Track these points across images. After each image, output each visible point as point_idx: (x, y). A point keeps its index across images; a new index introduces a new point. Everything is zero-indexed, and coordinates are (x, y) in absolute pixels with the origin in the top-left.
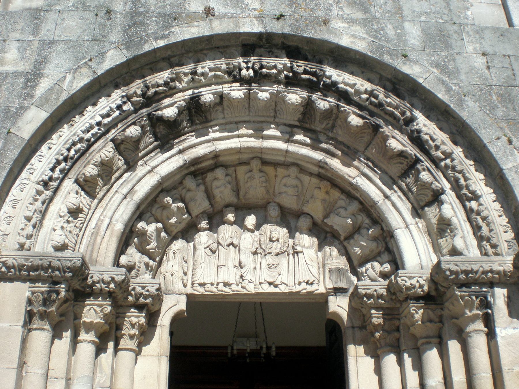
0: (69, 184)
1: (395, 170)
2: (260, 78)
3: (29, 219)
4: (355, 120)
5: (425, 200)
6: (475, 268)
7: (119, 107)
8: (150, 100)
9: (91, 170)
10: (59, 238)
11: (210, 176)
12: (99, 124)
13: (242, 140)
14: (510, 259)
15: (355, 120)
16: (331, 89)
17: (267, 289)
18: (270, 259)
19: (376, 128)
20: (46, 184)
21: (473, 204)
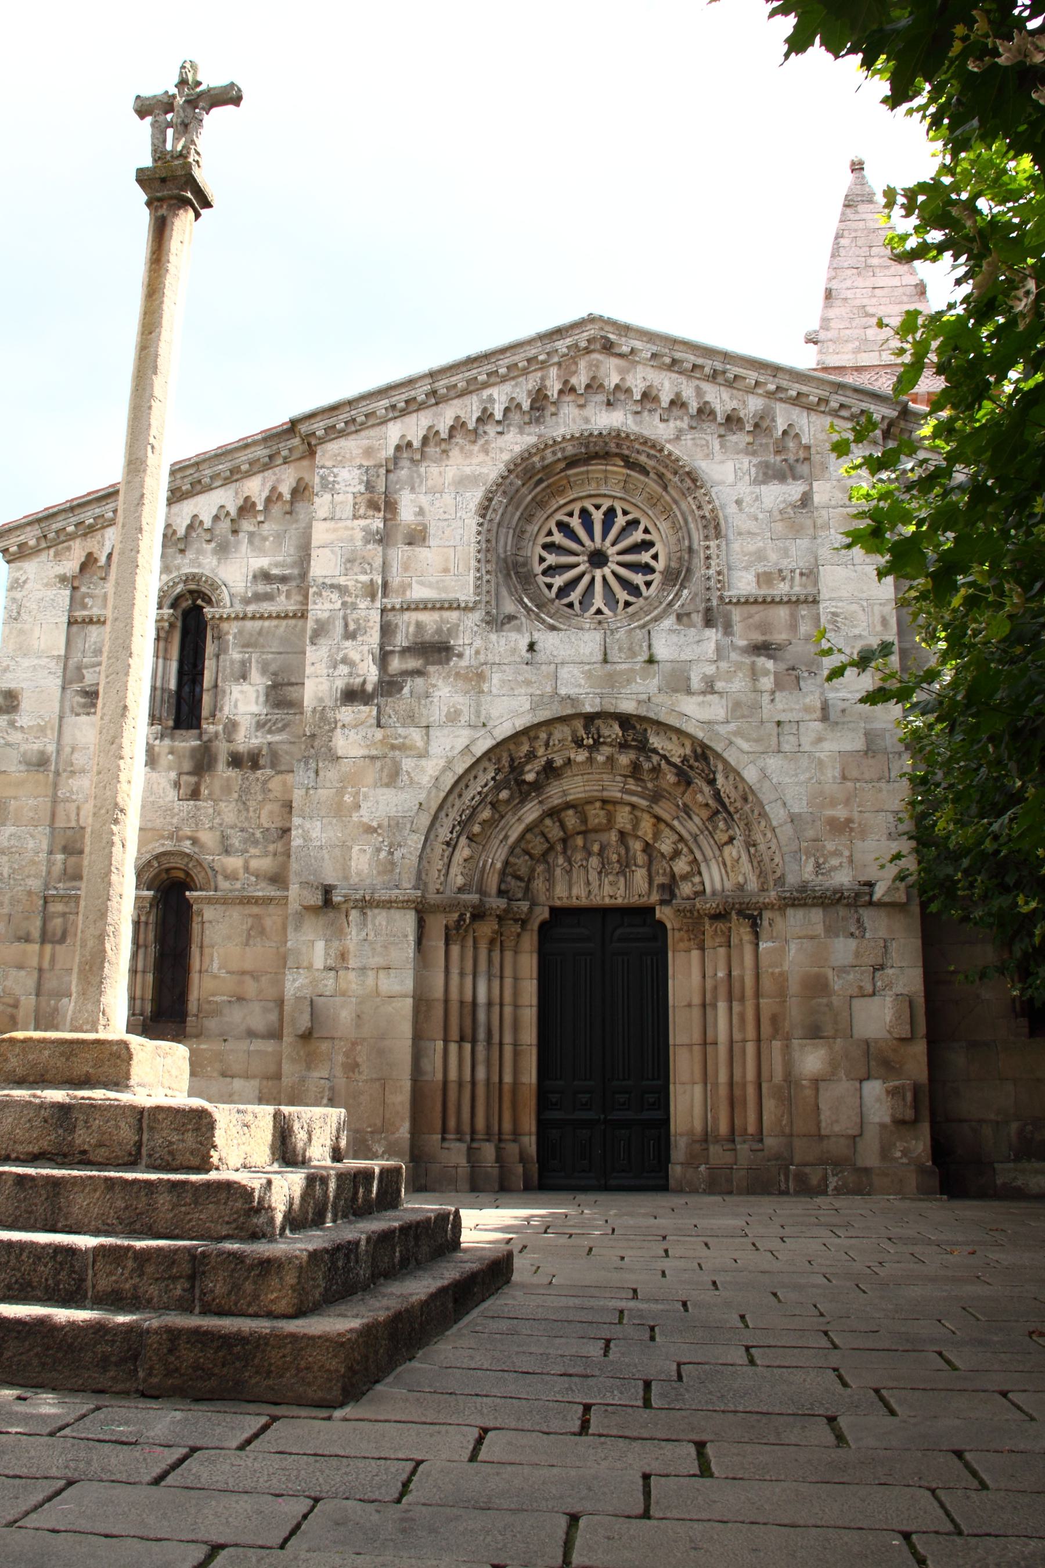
0: (463, 840)
3: (439, 871)
4: (671, 778)
6: (747, 900)
7: (493, 778)
8: (516, 768)
9: (476, 829)
10: (460, 881)
11: (563, 814)
12: (480, 793)
14: (773, 893)
16: (655, 751)
17: (607, 901)
18: (611, 878)
19: (689, 783)
20: (448, 844)
21: (752, 850)
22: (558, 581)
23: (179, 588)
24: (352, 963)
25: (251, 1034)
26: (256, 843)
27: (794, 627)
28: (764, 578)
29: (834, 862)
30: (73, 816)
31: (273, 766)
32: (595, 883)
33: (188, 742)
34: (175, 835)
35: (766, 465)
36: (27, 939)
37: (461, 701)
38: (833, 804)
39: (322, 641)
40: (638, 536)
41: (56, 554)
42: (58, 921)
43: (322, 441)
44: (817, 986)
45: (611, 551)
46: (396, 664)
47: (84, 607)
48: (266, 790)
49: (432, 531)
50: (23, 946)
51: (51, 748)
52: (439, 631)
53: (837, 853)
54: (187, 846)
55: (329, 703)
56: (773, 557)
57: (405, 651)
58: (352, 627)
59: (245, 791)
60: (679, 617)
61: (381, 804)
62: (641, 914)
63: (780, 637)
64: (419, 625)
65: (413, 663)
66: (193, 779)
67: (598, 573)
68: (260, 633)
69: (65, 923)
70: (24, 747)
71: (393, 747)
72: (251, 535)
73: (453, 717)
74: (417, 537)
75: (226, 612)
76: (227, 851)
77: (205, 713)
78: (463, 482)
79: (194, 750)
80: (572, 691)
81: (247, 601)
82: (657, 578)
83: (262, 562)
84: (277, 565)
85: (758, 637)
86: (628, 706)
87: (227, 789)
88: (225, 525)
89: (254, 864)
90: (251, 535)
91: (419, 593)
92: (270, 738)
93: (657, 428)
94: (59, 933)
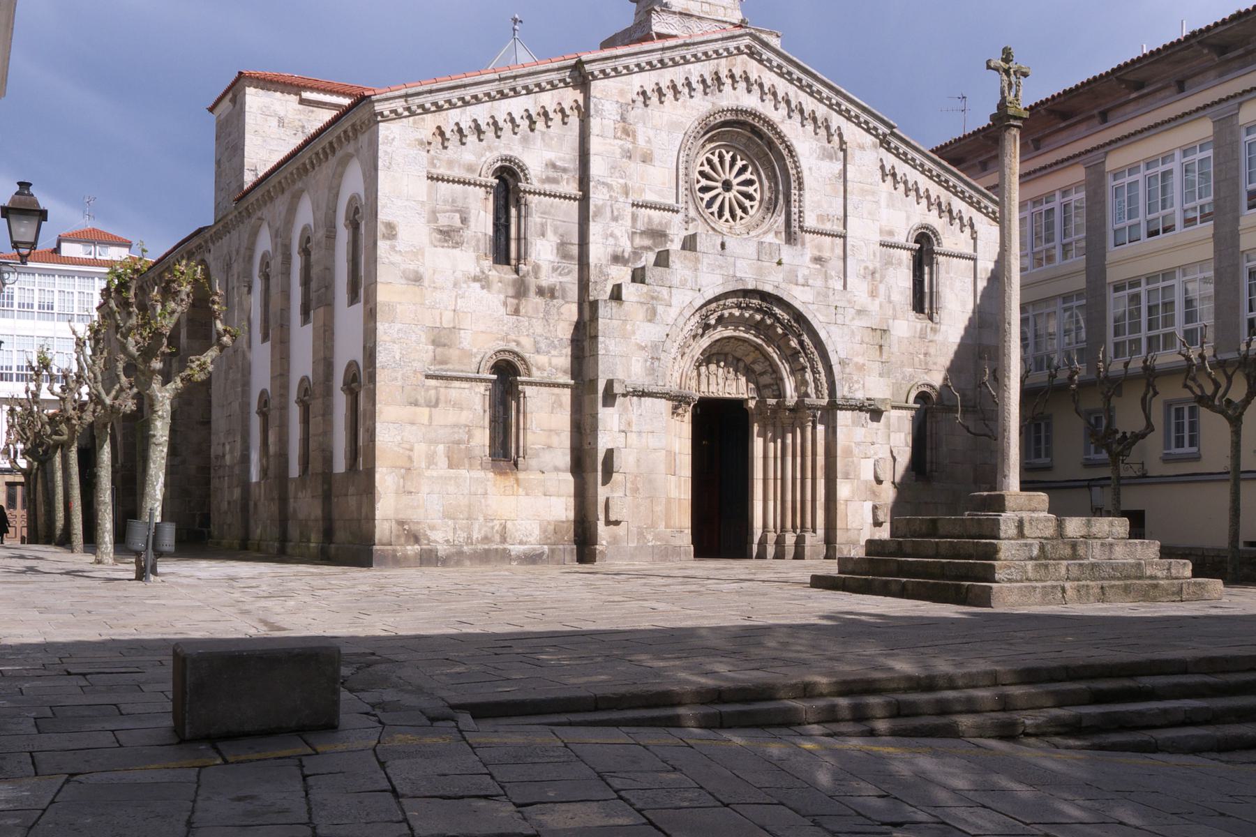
1: (789, 352)
2: (748, 307)
4: (780, 331)
5: (798, 370)
13: (729, 332)
15: (780, 331)
16: (774, 316)
22: (707, 196)
23: (499, 164)
24: (634, 429)
25: (557, 469)
26: (555, 347)
27: (832, 250)
28: (821, 218)
29: (856, 386)
30: (438, 319)
31: (563, 298)
32: (722, 384)
33: (506, 273)
34: (505, 338)
35: (824, 149)
36: (416, 404)
37: (688, 274)
38: (858, 355)
39: (598, 219)
40: (747, 176)
41: (415, 123)
42: (433, 392)
43: (595, 78)
44: (849, 452)
45: (735, 182)
46: (639, 241)
47: (434, 166)
48: (560, 314)
49: (655, 155)
50: (413, 409)
51: (421, 270)
52: (660, 223)
53: (858, 382)
54: (513, 346)
55: (604, 262)
56: (825, 206)
57: (643, 233)
58: (616, 213)
59: (547, 312)
60: (776, 233)
61: (647, 333)
62: (737, 405)
63: (826, 255)
64: (649, 217)
65: (647, 242)
66: (515, 301)
67: (727, 195)
68: (551, 206)
69: (438, 394)
70: (403, 266)
71: (653, 298)
72: (543, 133)
73: (683, 283)
74: (647, 159)
75: (528, 187)
76: (538, 352)
77: (513, 254)
78: (673, 126)
79: (515, 281)
80: (743, 275)
81: (543, 181)
82: (756, 203)
83: (551, 155)
84: (560, 159)
85: (817, 254)
86: (768, 288)
87: (536, 310)
88: (524, 124)
89: (555, 361)
90: (543, 133)
91: (650, 197)
92: (561, 279)
93: (777, 116)
94: (434, 400)
